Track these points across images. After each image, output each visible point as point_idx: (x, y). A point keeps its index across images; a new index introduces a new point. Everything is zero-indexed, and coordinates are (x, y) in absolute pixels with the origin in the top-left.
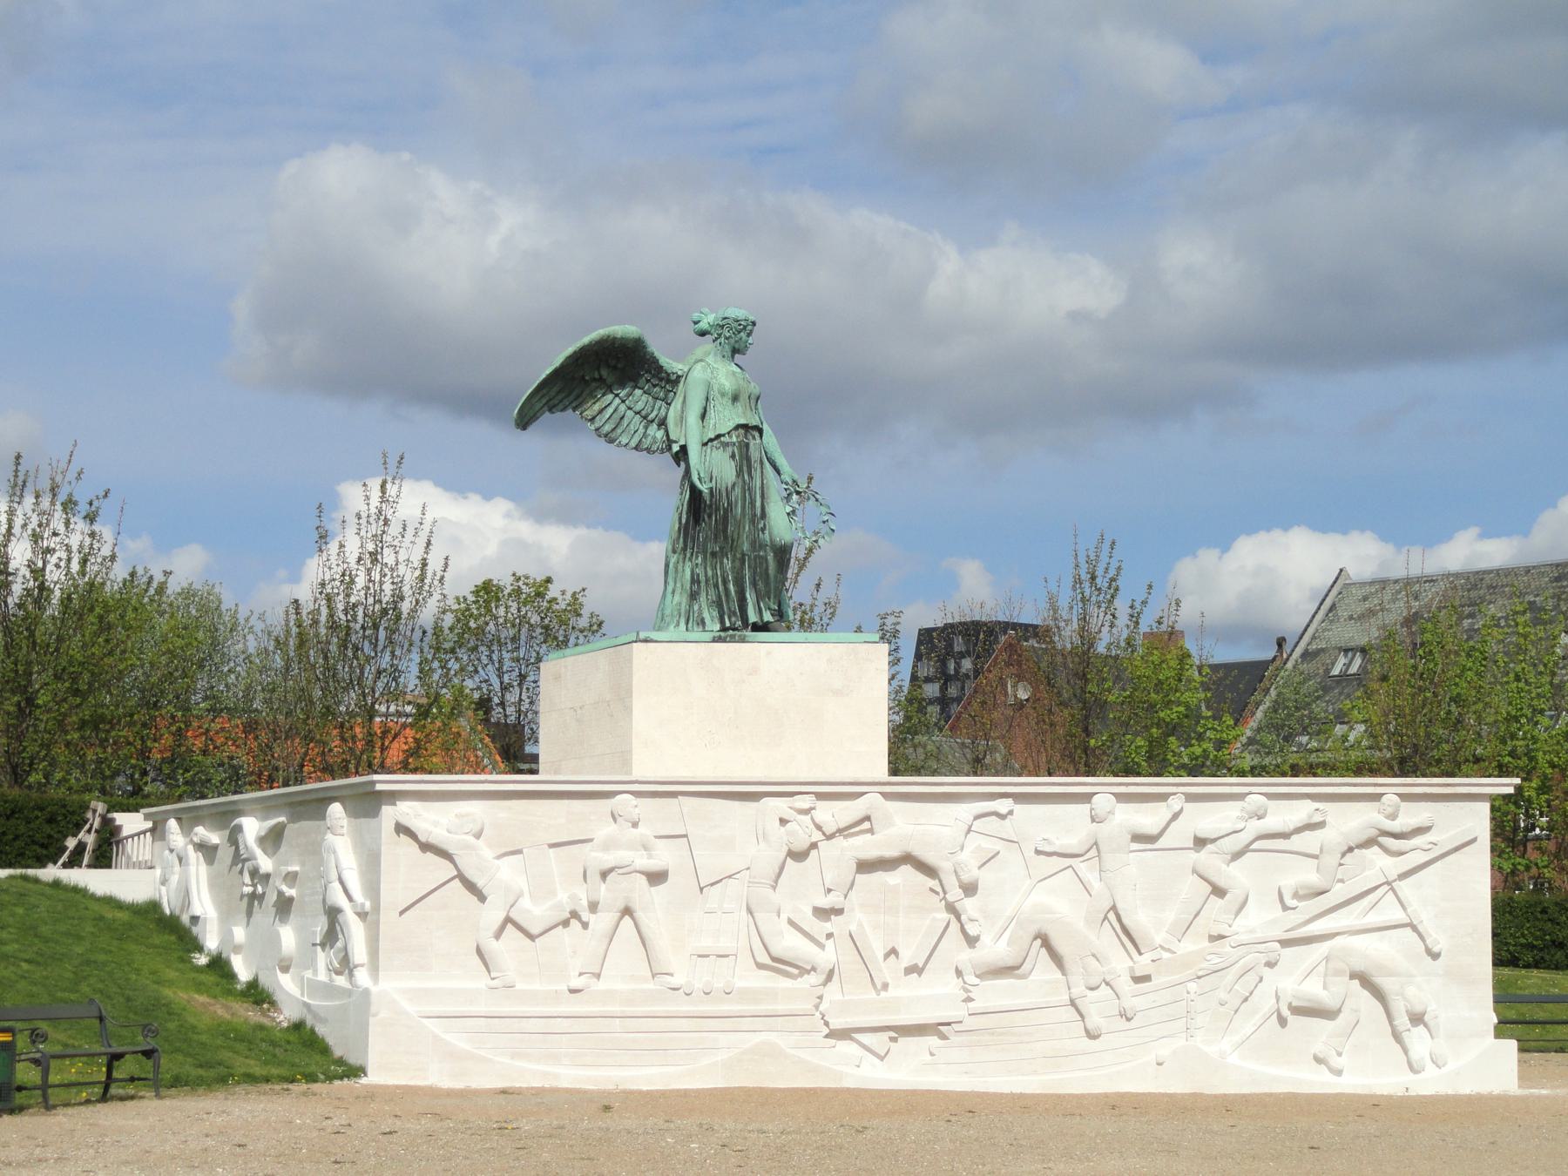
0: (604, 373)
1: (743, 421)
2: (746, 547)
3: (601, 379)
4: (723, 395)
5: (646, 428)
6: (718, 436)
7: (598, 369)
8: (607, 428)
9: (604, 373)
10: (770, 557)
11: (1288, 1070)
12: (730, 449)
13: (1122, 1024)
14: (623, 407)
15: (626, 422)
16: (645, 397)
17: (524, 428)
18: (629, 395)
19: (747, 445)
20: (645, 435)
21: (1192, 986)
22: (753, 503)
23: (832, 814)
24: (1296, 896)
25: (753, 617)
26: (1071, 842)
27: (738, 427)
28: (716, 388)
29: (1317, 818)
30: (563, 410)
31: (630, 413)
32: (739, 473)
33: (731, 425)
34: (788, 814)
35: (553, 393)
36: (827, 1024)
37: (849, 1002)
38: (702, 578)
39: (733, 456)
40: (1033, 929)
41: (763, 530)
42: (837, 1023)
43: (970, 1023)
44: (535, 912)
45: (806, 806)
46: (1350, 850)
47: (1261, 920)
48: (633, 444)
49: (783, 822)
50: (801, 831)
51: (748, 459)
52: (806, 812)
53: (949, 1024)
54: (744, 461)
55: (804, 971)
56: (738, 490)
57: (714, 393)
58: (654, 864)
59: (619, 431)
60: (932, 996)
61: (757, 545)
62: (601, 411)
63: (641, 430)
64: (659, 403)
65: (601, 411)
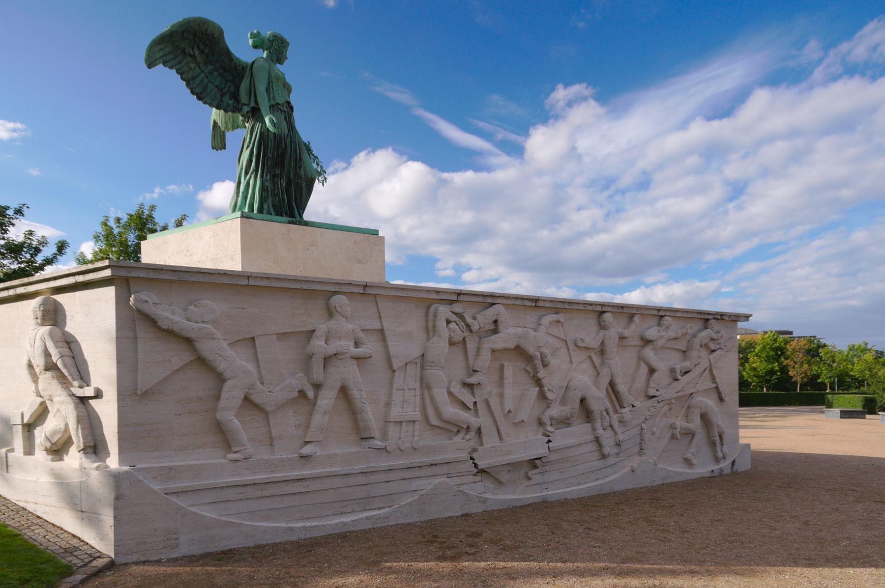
2: (292, 175)
3: (193, 56)
5: (222, 96)
8: (198, 90)
9: (197, 52)
14: (206, 80)
16: (219, 78)
18: (211, 73)
30: (171, 68)
31: (210, 85)
36: (476, 465)
39: (285, 119)
41: (300, 168)
42: (482, 464)
43: (553, 457)
49: (448, 322)
56: (288, 141)
61: (297, 174)
62: (194, 78)
64: (229, 84)
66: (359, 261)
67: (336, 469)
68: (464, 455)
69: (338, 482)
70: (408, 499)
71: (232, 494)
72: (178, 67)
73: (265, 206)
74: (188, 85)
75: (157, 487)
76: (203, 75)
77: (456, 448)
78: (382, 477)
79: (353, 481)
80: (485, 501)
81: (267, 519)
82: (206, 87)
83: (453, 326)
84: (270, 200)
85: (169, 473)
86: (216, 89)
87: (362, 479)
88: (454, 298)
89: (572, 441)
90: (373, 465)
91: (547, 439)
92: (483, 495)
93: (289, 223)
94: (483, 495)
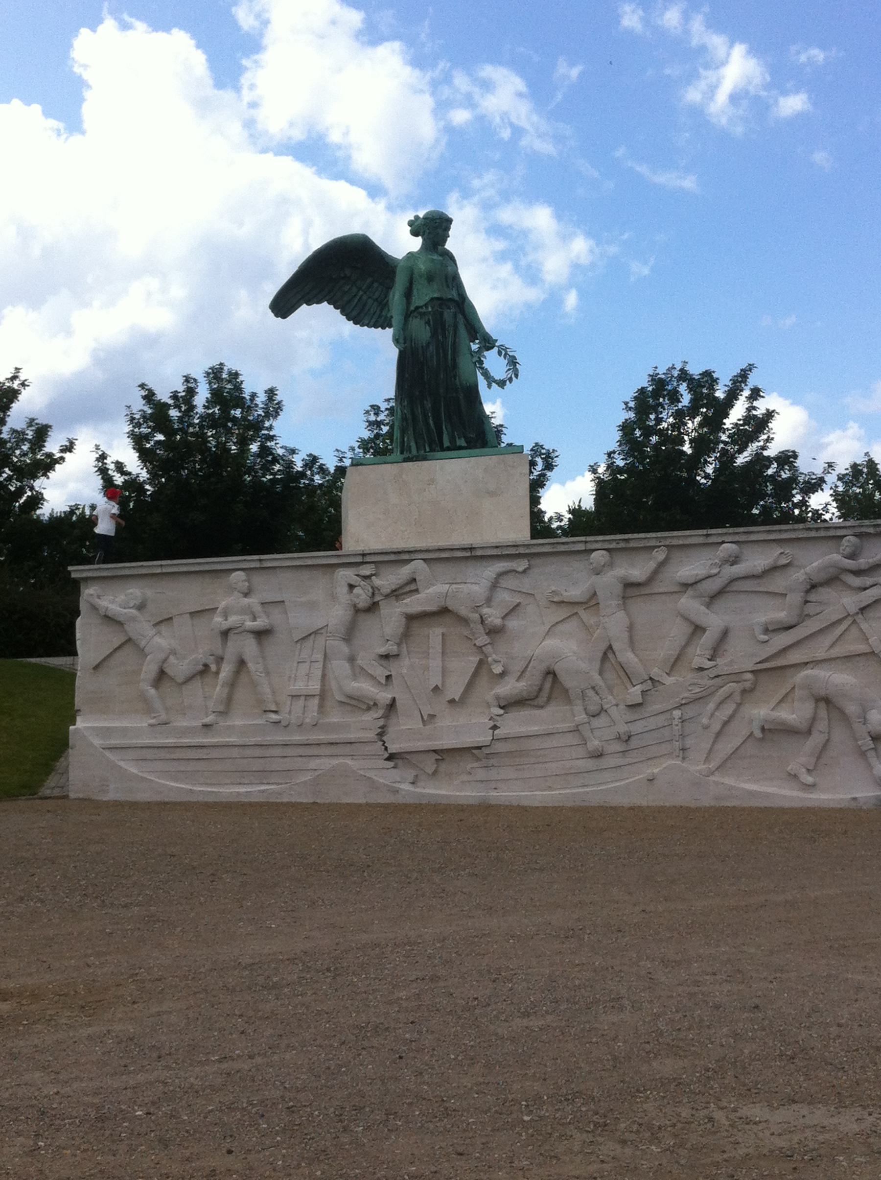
0: (348, 272)
1: (436, 295)
4: (421, 276)
6: (417, 308)
9: (348, 272)
10: (461, 396)
11: (765, 786)
12: (427, 318)
13: (618, 747)
15: (367, 308)
17: (284, 316)
19: (442, 314)
20: (380, 316)
21: (677, 713)
22: (446, 355)
23: (388, 580)
24: (766, 631)
25: (446, 443)
26: (576, 592)
27: (432, 299)
28: (416, 271)
29: (784, 561)
30: (319, 302)
31: (370, 301)
32: (434, 334)
33: (427, 298)
34: (355, 580)
36: (386, 749)
37: (406, 734)
38: (409, 416)
40: (543, 667)
41: (455, 376)
43: (499, 747)
44: (180, 668)
45: (368, 573)
46: (813, 587)
47: (742, 655)
48: (372, 323)
49: (351, 587)
50: (362, 596)
52: (366, 578)
53: (479, 748)
54: (438, 327)
55: (369, 708)
57: (416, 275)
58: (261, 623)
59: (362, 315)
60: (469, 727)
62: (349, 302)
63: (378, 312)
65: (349, 302)
66: (492, 494)
67: (233, 740)
68: (371, 735)
69: (235, 753)
70: (308, 777)
71: (149, 754)
72: (327, 298)
73: (406, 439)
74: (343, 313)
75: (97, 742)
76: (361, 293)
77: (362, 726)
78: (277, 752)
79: (248, 752)
80: (396, 791)
81: (176, 781)
82: (365, 305)
83: (356, 591)
84: (411, 432)
85: (106, 732)
86: (376, 304)
87: (258, 752)
88: (359, 559)
89: (534, 729)
90: (269, 739)
91: (492, 723)
92: (397, 785)
93: (406, 460)
94: (397, 785)
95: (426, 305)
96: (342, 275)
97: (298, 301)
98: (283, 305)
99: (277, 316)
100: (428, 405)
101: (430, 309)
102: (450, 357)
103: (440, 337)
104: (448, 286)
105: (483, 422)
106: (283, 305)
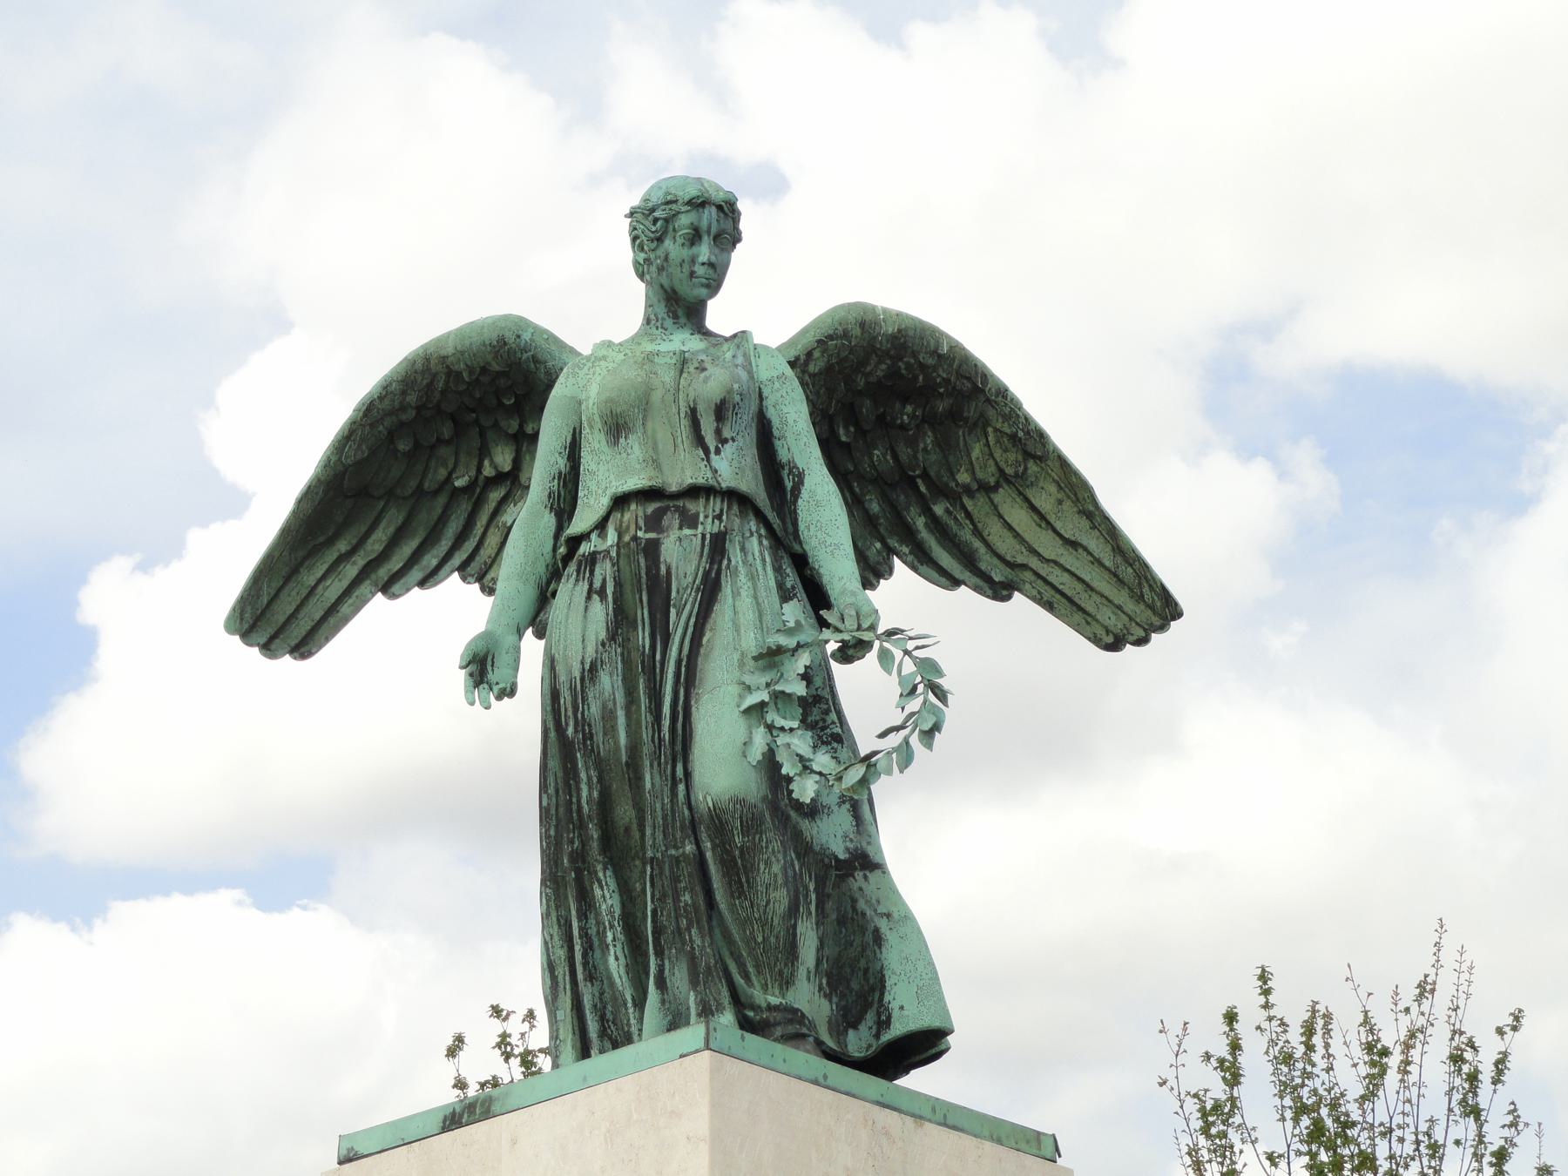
1: (633, 483)
7: (484, 452)
19: (652, 550)
27: (620, 502)
35: (376, 544)
51: (658, 587)
56: (609, 683)
72: (458, 559)
95: (601, 526)
96: (488, 471)
97: (347, 592)
98: (285, 608)
99: (268, 649)
100: (607, 898)
101: (612, 536)
102: (666, 709)
103: (643, 637)
104: (699, 441)
105: (878, 939)
106: (285, 608)
